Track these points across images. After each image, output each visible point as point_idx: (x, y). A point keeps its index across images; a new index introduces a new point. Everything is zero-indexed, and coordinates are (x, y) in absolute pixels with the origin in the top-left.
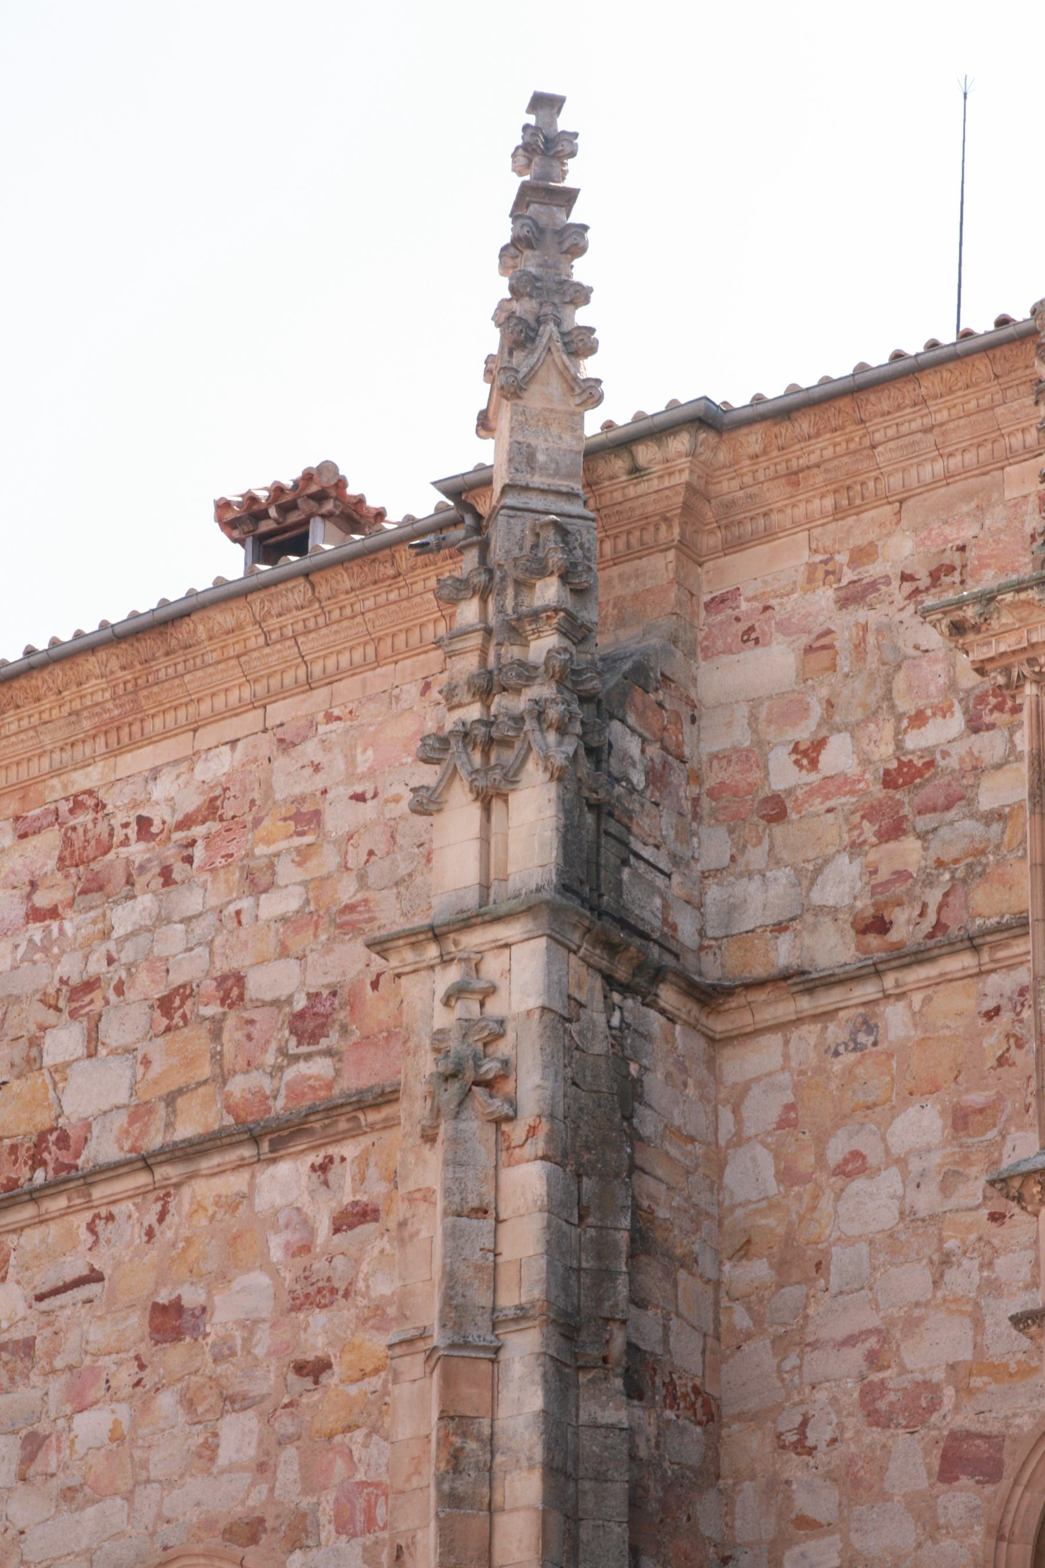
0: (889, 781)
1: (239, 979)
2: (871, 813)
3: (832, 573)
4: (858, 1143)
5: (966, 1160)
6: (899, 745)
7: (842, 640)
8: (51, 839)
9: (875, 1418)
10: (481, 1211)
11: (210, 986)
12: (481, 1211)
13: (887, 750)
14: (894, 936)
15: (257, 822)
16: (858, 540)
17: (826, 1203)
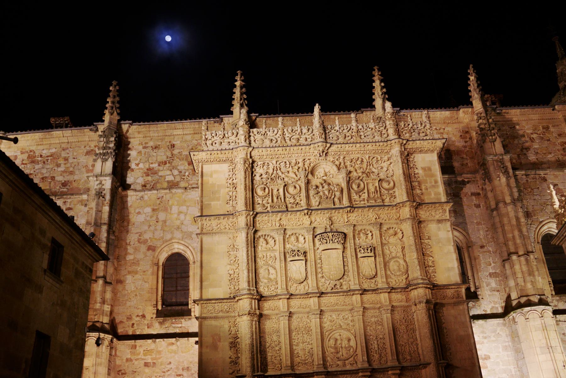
0: (147, 170)
1: (54, 177)
2: (145, 173)
3: (142, 144)
4: (140, 211)
5: (154, 215)
6: (149, 166)
7: (143, 152)
8: (27, 155)
9: (139, 242)
10: (100, 211)
11: (50, 178)
12: (100, 211)
13: (148, 166)
14: (147, 188)
15: (59, 158)
16: (146, 141)
17: (135, 217)
